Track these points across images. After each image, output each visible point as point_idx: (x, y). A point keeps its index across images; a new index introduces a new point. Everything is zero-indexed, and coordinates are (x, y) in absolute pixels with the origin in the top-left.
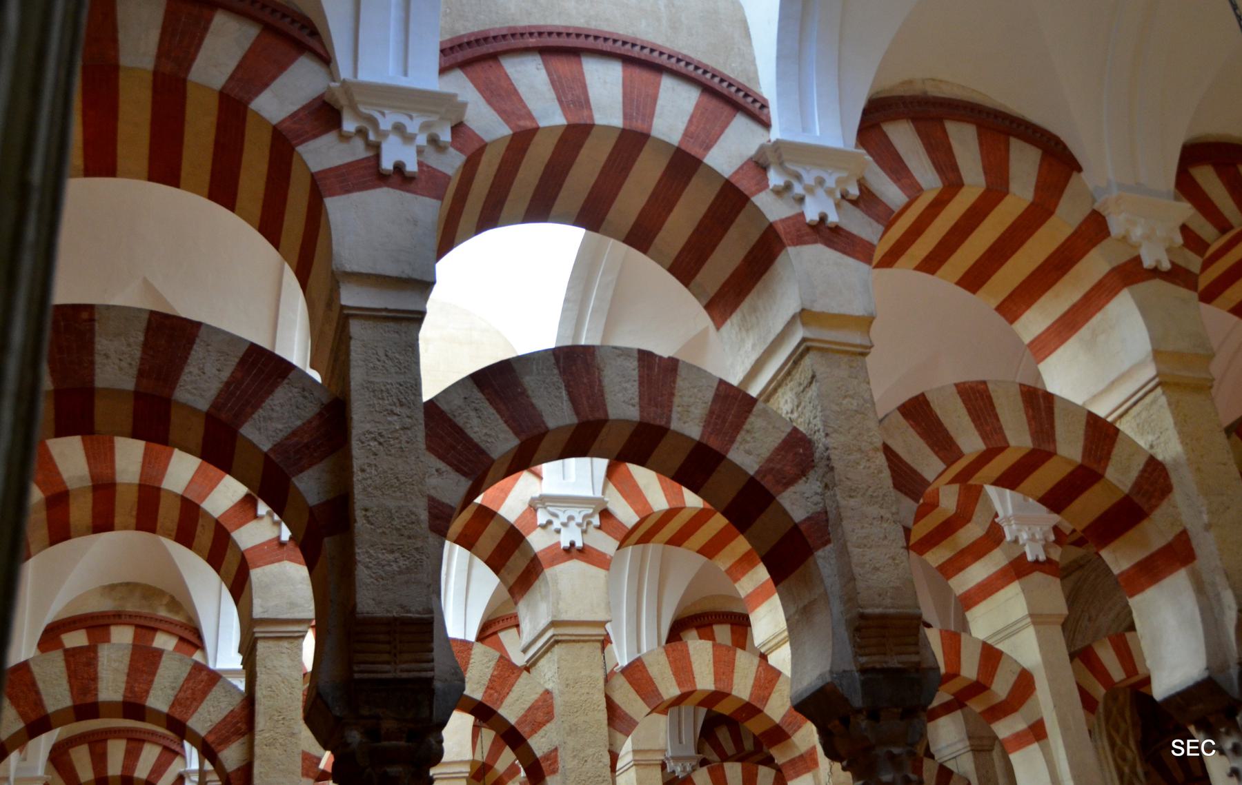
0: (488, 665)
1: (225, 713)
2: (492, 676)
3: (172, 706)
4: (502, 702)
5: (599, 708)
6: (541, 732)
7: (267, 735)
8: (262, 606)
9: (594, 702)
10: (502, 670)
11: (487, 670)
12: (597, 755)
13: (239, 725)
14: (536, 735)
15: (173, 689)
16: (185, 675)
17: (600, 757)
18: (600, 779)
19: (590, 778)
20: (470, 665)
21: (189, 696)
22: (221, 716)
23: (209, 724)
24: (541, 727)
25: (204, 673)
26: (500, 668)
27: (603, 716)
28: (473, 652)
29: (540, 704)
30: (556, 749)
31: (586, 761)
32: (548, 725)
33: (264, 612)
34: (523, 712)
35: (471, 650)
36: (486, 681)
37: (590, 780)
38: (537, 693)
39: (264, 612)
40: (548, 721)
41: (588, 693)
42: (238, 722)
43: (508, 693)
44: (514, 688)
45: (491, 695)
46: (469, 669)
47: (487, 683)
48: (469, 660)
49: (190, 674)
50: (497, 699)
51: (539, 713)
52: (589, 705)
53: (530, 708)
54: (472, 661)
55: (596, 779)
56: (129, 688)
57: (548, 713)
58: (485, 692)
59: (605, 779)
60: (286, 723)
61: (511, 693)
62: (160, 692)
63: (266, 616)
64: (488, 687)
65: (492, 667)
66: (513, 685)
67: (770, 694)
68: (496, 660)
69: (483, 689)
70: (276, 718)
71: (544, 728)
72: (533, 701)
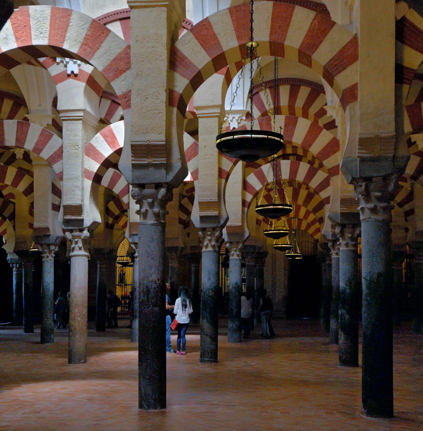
0: (84, 27)
2: (86, 35)
4: (93, 55)
5: (161, 58)
6: (122, 77)
9: (157, 54)
10: (94, 31)
11: (82, 31)
12: (156, 93)
14: (118, 79)
17: (158, 95)
18: (156, 111)
19: (149, 110)
20: (69, 28)
24: (122, 73)
26: (92, 30)
27: (164, 64)
28: (71, 18)
29: (123, 56)
31: (147, 98)
34: (109, 62)
35: (70, 16)
36: (81, 39)
37: (149, 113)
38: (120, 48)
40: (127, 69)
41: (153, 47)
43: (98, 48)
44: (102, 45)
45: (85, 50)
46: (68, 30)
47: (82, 41)
48: (69, 24)
50: (90, 53)
51: (121, 63)
52: (153, 55)
53: (115, 59)
54: (71, 24)
55: (154, 112)
58: (81, 47)
59: (162, 111)
61: (100, 48)
64: (83, 44)
65: (86, 28)
66: (102, 42)
67: (321, 42)
68: (90, 24)
69: (79, 45)
71: (125, 74)
72: (117, 54)
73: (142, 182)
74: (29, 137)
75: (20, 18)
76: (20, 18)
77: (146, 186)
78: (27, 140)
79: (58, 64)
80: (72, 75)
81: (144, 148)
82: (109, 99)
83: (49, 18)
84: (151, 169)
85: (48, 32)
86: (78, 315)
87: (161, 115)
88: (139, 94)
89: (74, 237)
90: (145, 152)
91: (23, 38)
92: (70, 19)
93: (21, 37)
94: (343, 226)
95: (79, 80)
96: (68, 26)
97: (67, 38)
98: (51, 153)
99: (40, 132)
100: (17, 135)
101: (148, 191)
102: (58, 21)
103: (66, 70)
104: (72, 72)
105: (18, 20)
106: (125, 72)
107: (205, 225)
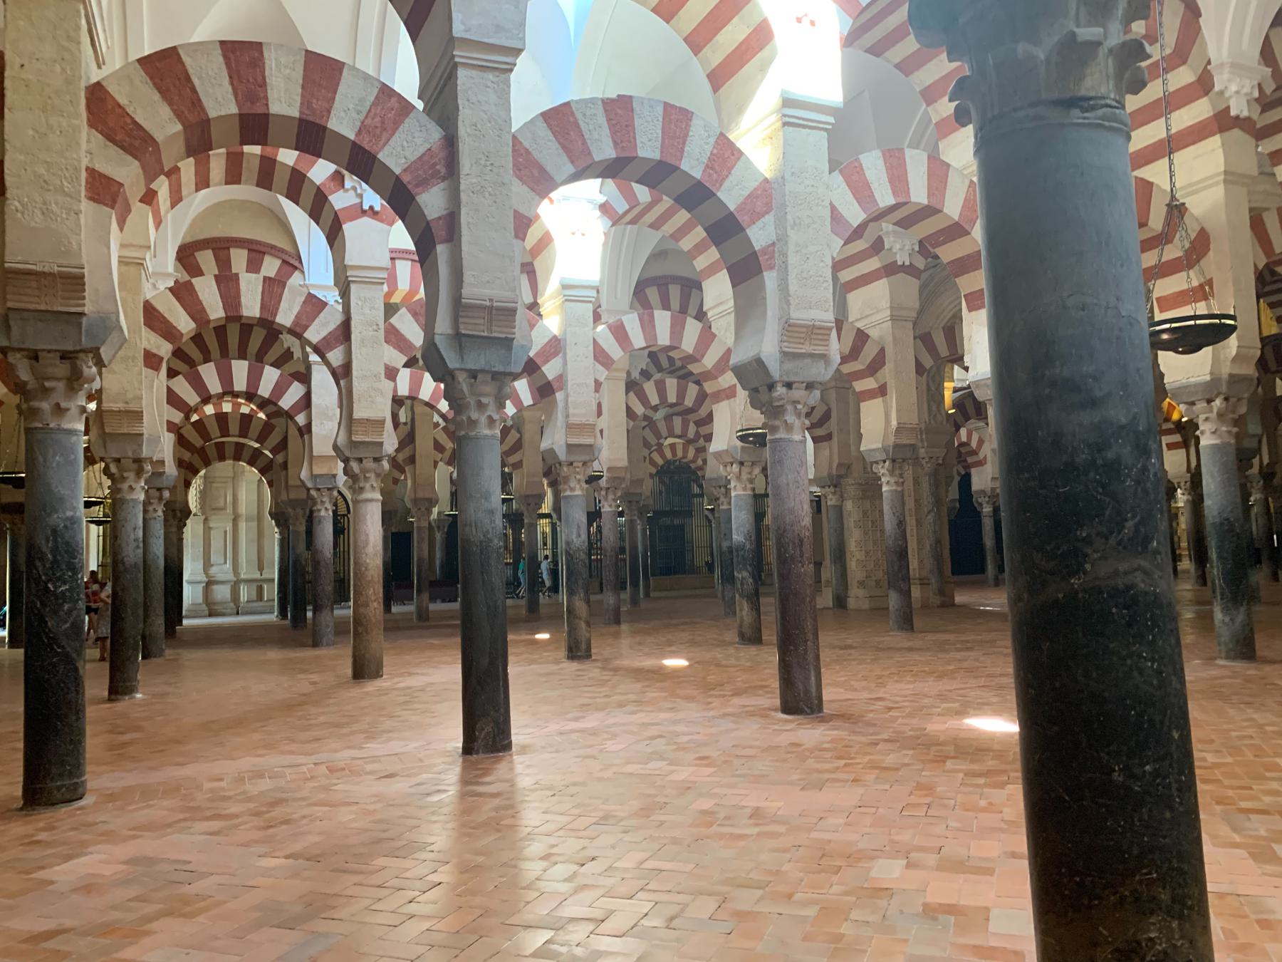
1: (422, 150)
3: (359, 133)
7: (474, 181)
8: (462, 23)
13: (438, 167)
15: (359, 112)
16: (372, 99)
21: (379, 125)
22: (418, 154)
23: (404, 160)
25: (394, 100)
30: (773, 244)
32: (767, 216)
33: (466, 31)
39: (466, 31)
40: (767, 213)
42: (435, 164)
49: (377, 98)
50: (716, 181)
53: (749, 195)
54: (691, 133)
56: (306, 103)
57: (767, 204)
60: (495, 170)
62: (343, 114)
63: (467, 36)
64: (707, 165)
69: (702, 167)
70: (483, 163)
71: (763, 219)
73: (792, 379)
74: (284, 305)
75: (619, 111)
76: (619, 111)
77: (794, 386)
78: (280, 309)
79: (347, 190)
80: (370, 212)
81: (805, 330)
82: (279, 258)
83: (661, 119)
84: (808, 361)
85: (660, 139)
86: (373, 598)
87: (825, 285)
88: (797, 252)
89: (364, 471)
90: (802, 335)
91: (624, 144)
92: (690, 126)
93: (622, 142)
94: (742, 464)
95: (382, 221)
96: (686, 135)
97: (685, 154)
98: (324, 334)
99: (303, 299)
100: (262, 299)
101: (798, 393)
102: (673, 126)
103: (362, 202)
104: (371, 208)
105: (616, 114)
106: (763, 216)
107: (572, 459)
